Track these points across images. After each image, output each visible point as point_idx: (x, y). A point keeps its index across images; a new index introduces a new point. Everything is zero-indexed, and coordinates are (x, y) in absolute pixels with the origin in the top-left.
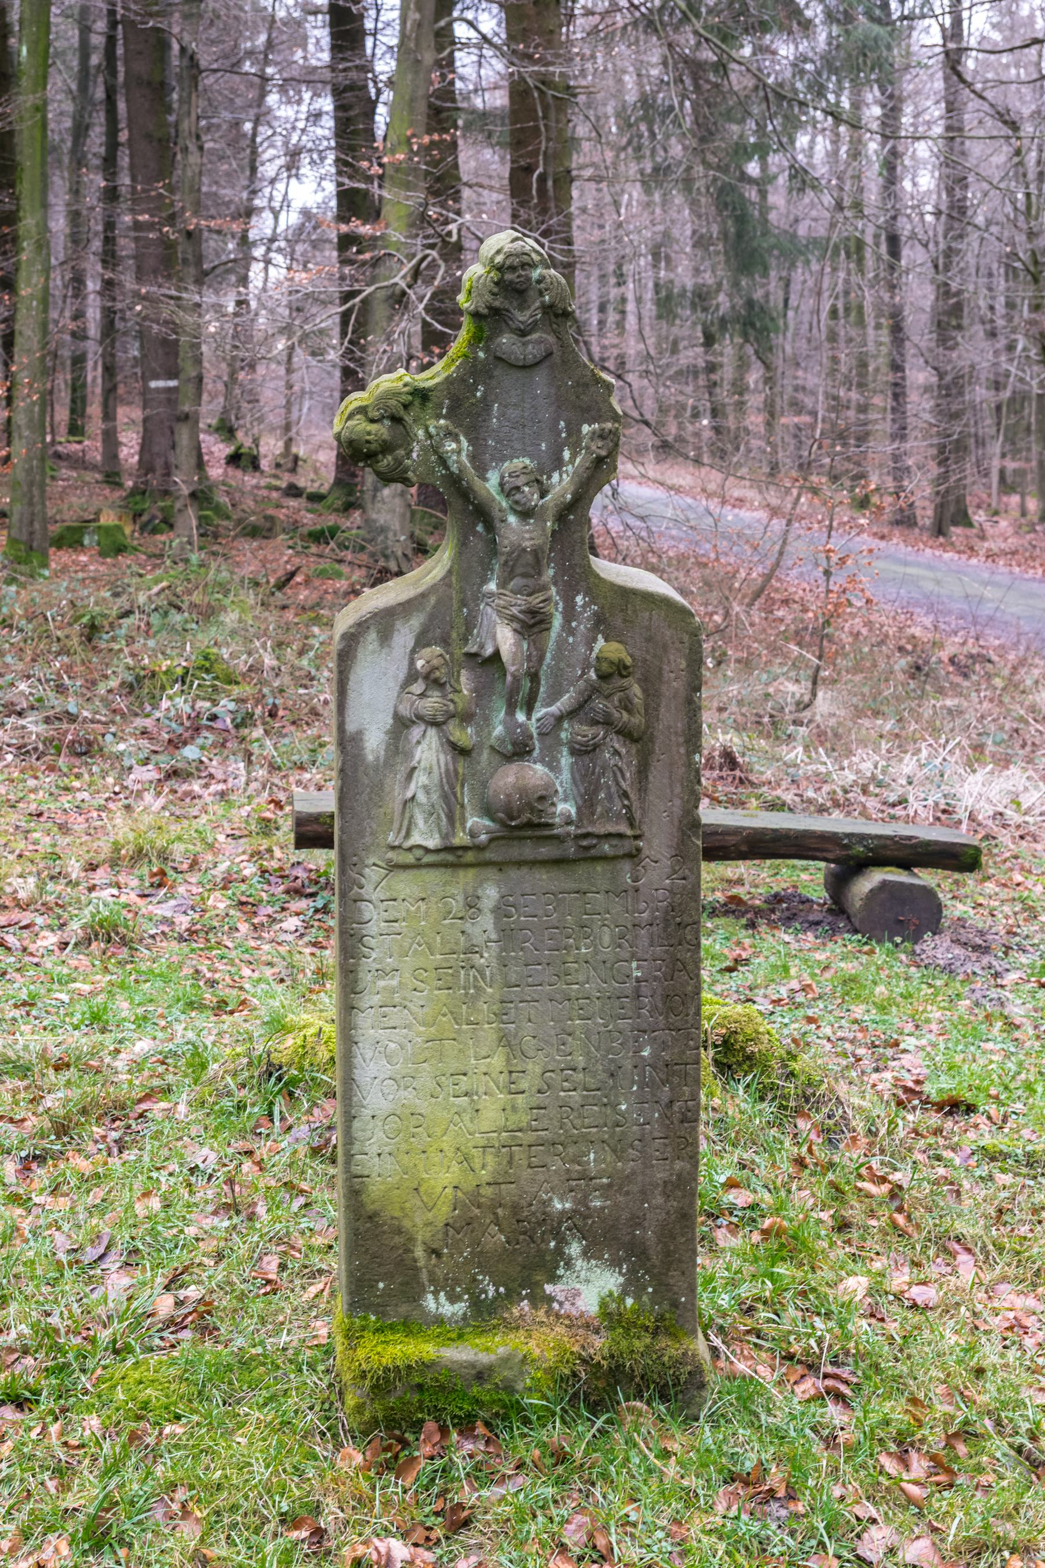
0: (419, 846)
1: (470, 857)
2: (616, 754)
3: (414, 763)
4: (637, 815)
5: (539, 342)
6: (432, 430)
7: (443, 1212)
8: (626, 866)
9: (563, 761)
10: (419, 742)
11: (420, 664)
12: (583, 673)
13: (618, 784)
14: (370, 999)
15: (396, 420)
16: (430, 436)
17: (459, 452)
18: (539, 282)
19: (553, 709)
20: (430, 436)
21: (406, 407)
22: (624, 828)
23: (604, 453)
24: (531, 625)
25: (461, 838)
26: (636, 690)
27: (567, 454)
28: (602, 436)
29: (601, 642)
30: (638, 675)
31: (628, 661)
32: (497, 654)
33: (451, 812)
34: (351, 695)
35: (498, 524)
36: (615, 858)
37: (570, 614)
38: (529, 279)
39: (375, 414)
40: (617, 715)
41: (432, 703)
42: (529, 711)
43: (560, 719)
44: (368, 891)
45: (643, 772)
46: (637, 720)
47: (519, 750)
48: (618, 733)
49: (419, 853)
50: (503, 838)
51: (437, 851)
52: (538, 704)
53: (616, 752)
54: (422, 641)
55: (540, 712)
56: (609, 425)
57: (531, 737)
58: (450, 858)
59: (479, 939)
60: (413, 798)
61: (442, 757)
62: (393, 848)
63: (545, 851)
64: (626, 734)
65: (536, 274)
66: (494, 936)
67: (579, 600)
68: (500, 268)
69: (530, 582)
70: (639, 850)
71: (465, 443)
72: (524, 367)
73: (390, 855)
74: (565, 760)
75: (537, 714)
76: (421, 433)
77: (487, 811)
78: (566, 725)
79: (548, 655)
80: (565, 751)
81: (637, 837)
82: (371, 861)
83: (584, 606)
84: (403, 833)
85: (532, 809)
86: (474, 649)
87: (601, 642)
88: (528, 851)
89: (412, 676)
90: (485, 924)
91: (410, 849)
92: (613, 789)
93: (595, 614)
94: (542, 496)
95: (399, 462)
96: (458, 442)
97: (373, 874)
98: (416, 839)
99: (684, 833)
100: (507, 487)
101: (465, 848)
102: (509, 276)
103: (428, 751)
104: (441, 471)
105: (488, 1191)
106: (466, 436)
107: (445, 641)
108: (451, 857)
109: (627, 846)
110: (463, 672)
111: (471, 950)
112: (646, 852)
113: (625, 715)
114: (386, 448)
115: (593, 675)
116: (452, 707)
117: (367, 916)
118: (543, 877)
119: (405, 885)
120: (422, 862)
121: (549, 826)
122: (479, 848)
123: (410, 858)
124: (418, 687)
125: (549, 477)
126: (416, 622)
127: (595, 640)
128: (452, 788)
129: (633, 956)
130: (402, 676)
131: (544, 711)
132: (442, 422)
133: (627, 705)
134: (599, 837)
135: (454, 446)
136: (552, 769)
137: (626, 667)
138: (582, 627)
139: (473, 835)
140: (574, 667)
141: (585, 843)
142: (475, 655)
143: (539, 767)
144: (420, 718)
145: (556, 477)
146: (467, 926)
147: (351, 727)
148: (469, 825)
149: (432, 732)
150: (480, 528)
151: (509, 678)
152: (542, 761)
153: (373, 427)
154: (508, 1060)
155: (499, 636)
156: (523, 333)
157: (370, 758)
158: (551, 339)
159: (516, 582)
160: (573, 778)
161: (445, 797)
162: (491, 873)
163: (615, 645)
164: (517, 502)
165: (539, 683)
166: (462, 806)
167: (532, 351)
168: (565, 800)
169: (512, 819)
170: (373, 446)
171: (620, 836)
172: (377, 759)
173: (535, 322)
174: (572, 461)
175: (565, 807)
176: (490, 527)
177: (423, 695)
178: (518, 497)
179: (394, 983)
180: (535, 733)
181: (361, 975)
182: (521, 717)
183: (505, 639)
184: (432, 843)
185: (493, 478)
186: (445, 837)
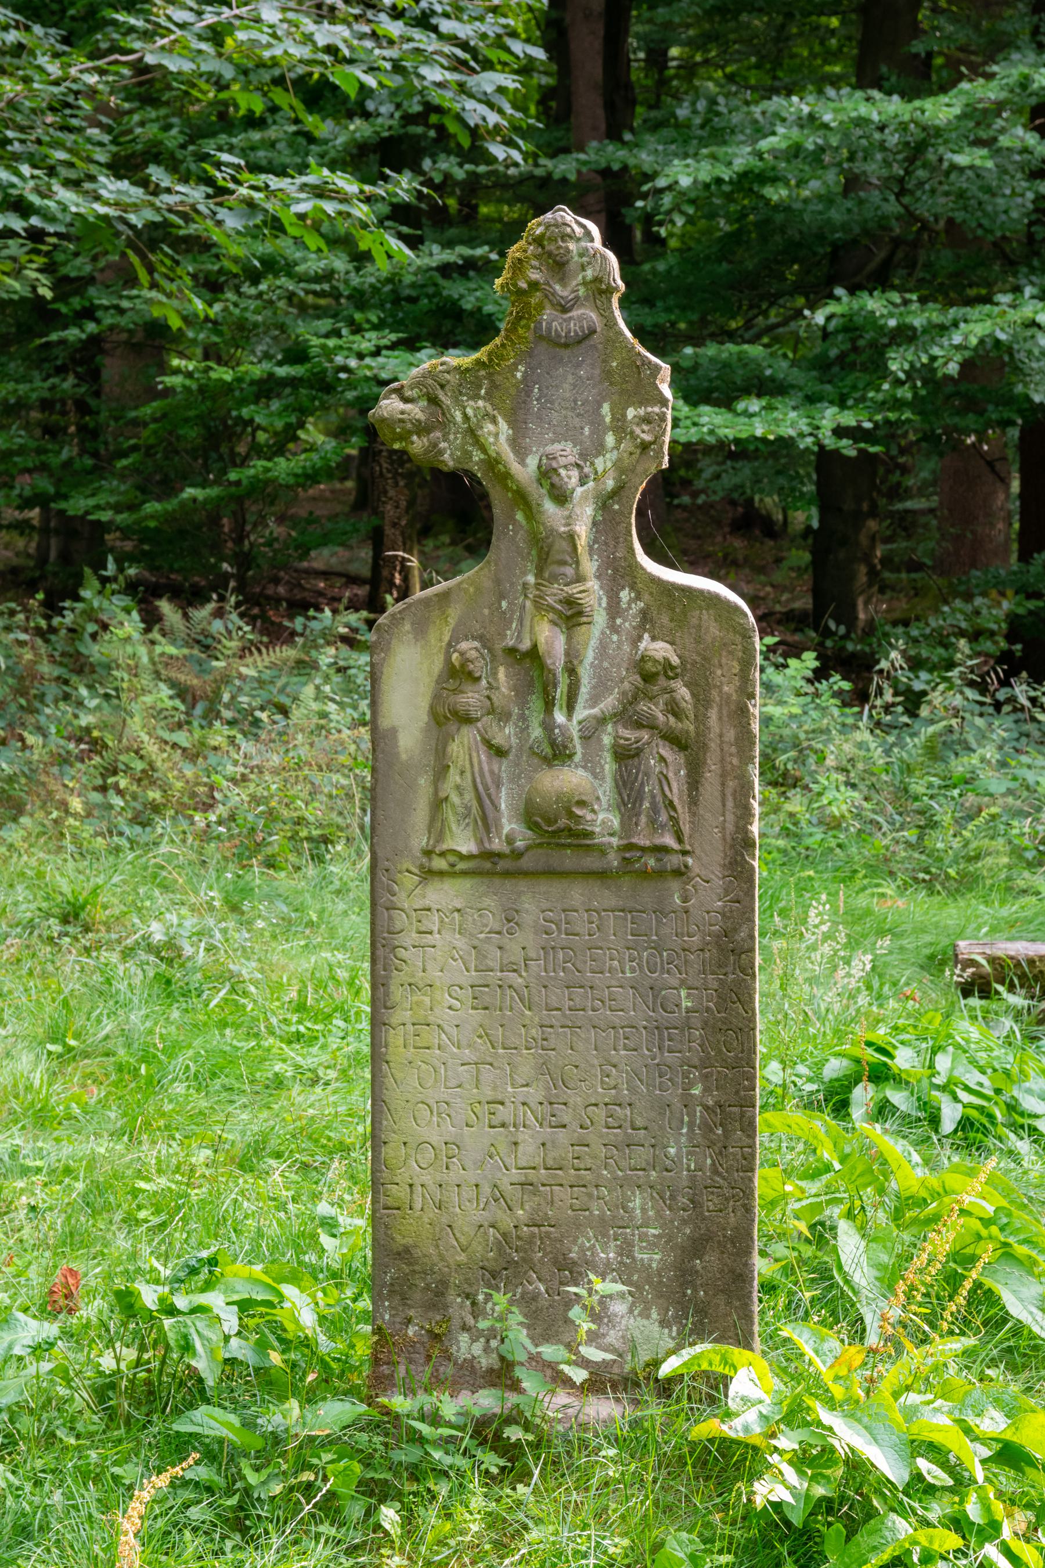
2: (665, 764)
4: (686, 829)
6: (470, 411)
8: (675, 885)
14: (400, 1015)
16: (466, 418)
17: (496, 435)
18: (581, 255)
19: (595, 711)
20: (466, 418)
23: (647, 438)
25: (497, 845)
26: (683, 692)
28: (647, 420)
31: (675, 660)
37: (614, 610)
40: (661, 717)
43: (602, 721)
44: (402, 899)
47: (557, 753)
49: (452, 859)
50: (540, 845)
51: (471, 857)
53: (662, 759)
55: (582, 712)
58: (488, 865)
67: (625, 595)
70: (686, 866)
71: (503, 425)
74: (609, 766)
76: (458, 416)
78: (610, 728)
81: (685, 853)
82: (405, 866)
83: (629, 603)
85: (571, 815)
88: (569, 859)
91: (442, 854)
92: (659, 799)
104: (477, 456)
106: (504, 417)
113: (672, 719)
117: (398, 926)
121: (589, 835)
127: (640, 638)
129: (683, 983)
132: (481, 403)
133: (674, 709)
136: (595, 776)
137: (672, 668)
138: (628, 624)
140: (619, 666)
143: (581, 772)
146: (506, 940)
150: (519, 516)
152: (585, 767)
157: (404, 757)
158: (593, 315)
170: (409, 426)
173: (577, 298)
180: (575, 734)
181: (392, 988)
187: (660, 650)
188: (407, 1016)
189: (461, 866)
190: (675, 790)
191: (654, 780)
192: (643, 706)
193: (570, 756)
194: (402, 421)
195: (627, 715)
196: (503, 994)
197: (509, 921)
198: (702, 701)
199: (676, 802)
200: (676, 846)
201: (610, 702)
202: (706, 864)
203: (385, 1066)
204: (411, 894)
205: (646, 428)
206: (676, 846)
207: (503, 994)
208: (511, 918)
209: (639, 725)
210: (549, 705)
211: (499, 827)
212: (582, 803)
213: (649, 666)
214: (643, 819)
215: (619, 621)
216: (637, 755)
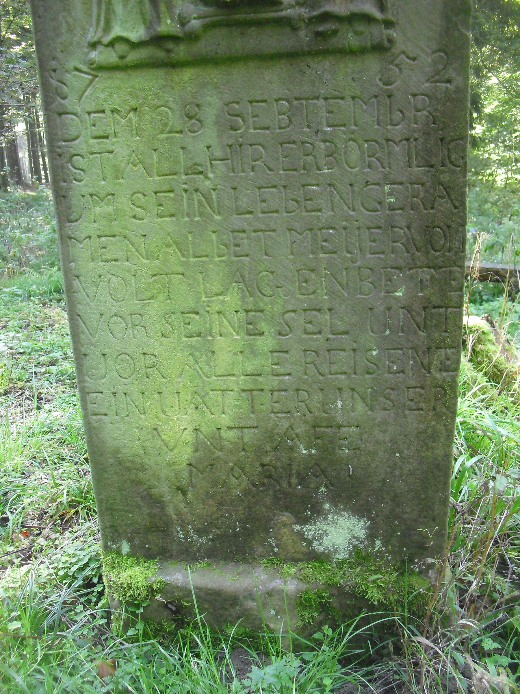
1: (181, 51)
7: (184, 454)
14: (85, 227)
25: (167, 26)
36: (363, 51)
51: (141, 44)
59: (202, 158)
63: (272, 41)
66: (218, 153)
70: (391, 41)
73: (94, 55)
81: (388, 24)
84: (102, 23)
90: (208, 139)
97: (75, 81)
98: (117, 31)
99: (447, 18)
105: (230, 435)
109: (378, 33)
112: (400, 46)
118: (273, 81)
119: (114, 91)
122: (191, 37)
134: (339, 19)
139: (183, 22)
146: (188, 139)
154: (243, 298)
162: (213, 75)
171: (368, 19)
179: (109, 209)
184: (137, 33)
186: (149, 26)
188: (92, 229)
189: (134, 56)
196: (191, 199)
197: (190, 118)
200: (378, 15)
203: (76, 282)
207: (191, 199)
208: (192, 116)
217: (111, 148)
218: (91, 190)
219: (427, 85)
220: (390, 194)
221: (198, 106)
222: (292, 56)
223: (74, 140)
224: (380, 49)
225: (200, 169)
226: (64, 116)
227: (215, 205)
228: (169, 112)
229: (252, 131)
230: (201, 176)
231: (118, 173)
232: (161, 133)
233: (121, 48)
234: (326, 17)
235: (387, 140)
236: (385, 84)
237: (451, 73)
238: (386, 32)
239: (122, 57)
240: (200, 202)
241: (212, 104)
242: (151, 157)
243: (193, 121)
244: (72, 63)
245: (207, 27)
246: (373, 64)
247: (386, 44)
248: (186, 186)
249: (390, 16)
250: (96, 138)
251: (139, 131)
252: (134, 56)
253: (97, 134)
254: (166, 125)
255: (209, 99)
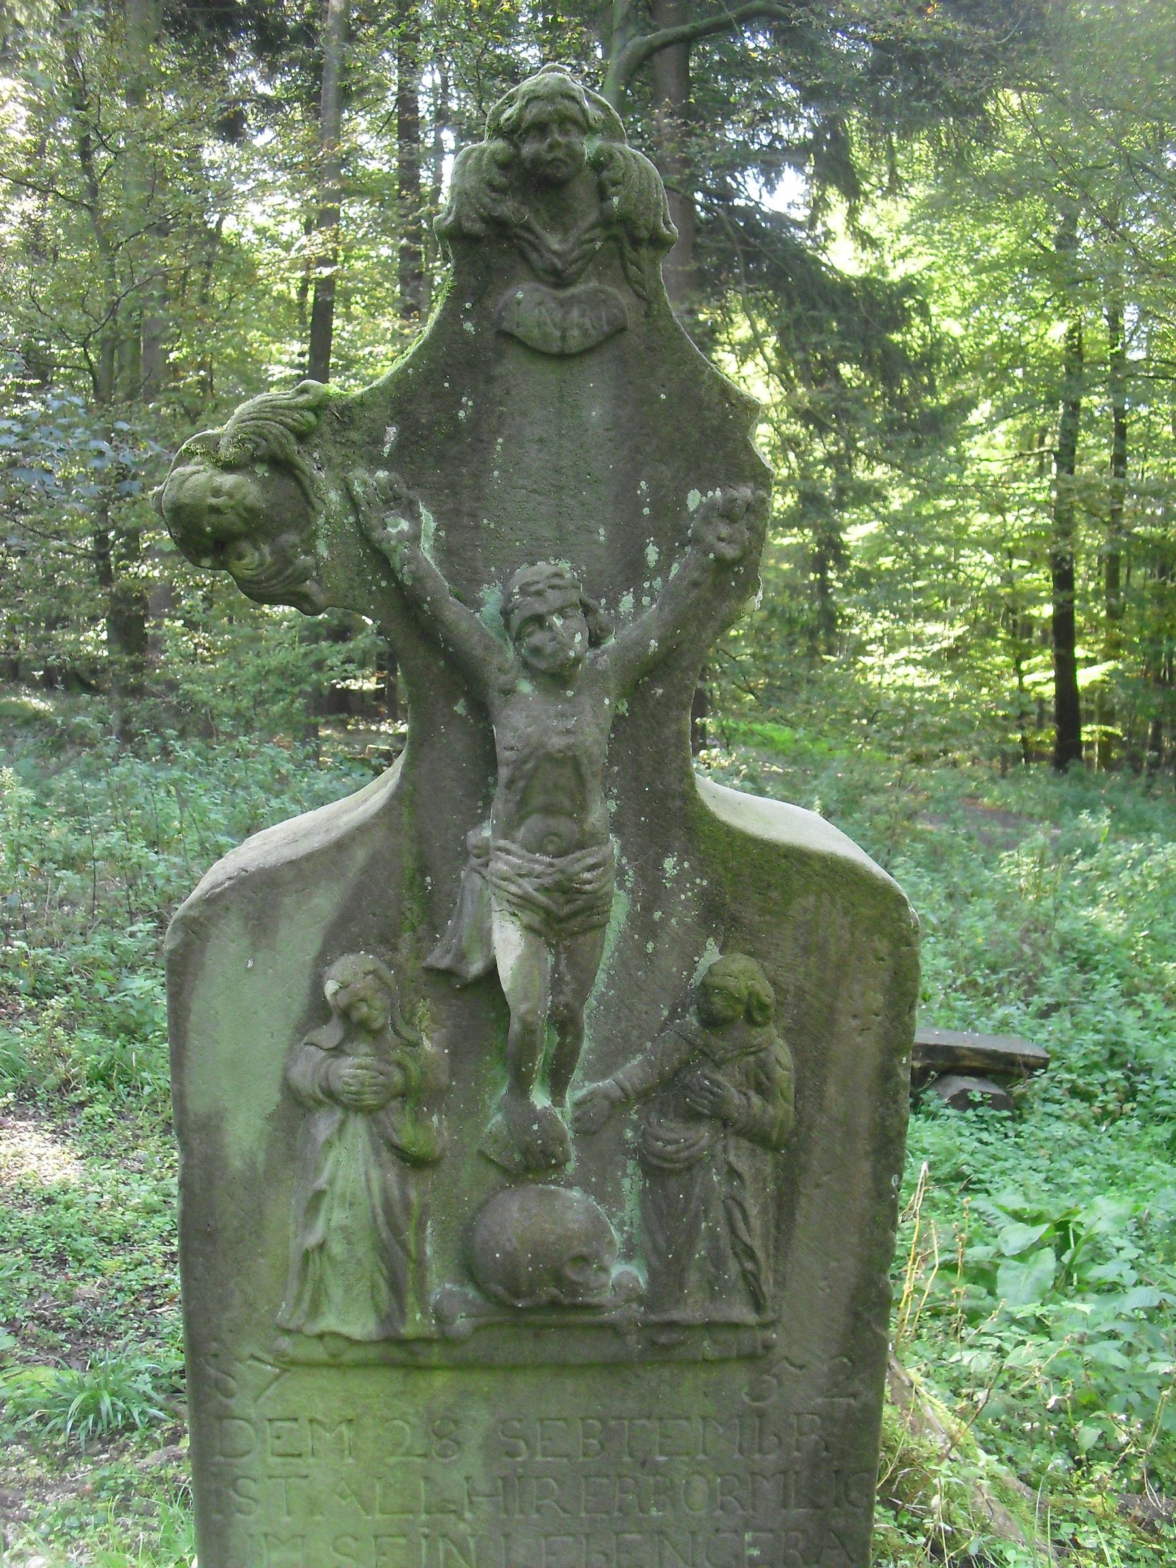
0: (335, 1335)
1: (435, 1354)
3: (321, 1183)
4: (768, 1288)
5: (594, 301)
6: (358, 489)
9: (626, 1183)
10: (329, 1144)
11: (330, 987)
12: (673, 1015)
13: (733, 1230)
15: (282, 466)
17: (415, 538)
21: (302, 437)
22: (742, 1313)
23: (730, 552)
24: (563, 920)
25: (416, 1323)
26: (782, 1052)
27: (652, 554)
28: (728, 513)
29: (711, 955)
30: (787, 1022)
31: (766, 992)
32: (491, 972)
33: (397, 1276)
34: (194, 1040)
35: (494, 697)
36: (723, 1361)
37: (651, 893)
38: (574, 155)
39: (227, 452)
40: (737, 1099)
41: (353, 1069)
42: (558, 1082)
44: (242, 1404)
45: (784, 1206)
46: (778, 1112)
47: (533, 1161)
48: (741, 1133)
51: (371, 1343)
52: (577, 1075)
53: (733, 1173)
54: (339, 939)
56: (745, 492)
57: (562, 1140)
58: (399, 1354)
60: (322, 1247)
61: (375, 1174)
62: (288, 1332)
64: (757, 1136)
65: (589, 147)
66: (483, 1486)
68: (512, 132)
69: (563, 825)
70: (768, 1347)
71: (428, 521)
72: (562, 357)
74: (630, 1183)
75: (572, 1096)
76: (334, 496)
77: (469, 1269)
79: (601, 977)
80: (631, 1166)
81: (764, 1326)
84: (305, 1305)
85: (558, 1279)
86: (445, 963)
87: (711, 955)
89: (319, 1011)
90: (467, 1468)
91: (321, 1336)
92: (725, 1243)
93: (703, 893)
94: (595, 641)
95: (284, 559)
96: (415, 518)
98: (329, 1322)
99: (857, 1316)
100: (516, 619)
101: (427, 1341)
102: (528, 149)
103: (349, 1164)
107: (387, 940)
108: (398, 1353)
110: (423, 1008)
111: (442, 1507)
112: (780, 1351)
113: (756, 1100)
114: (256, 525)
115: (692, 1020)
116: (397, 1077)
119: (319, 1396)
120: (341, 1356)
123: (319, 1352)
124: (330, 1034)
125: (614, 603)
126: (325, 901)
127: (699, 949)
128: (395, 1230)
129: (747, 1526)
130: (298, 1005)
131: (590, 1086)
132: (382, 474)
135: (404, 525)
136: (601, 1198)
137: (763, 1007)
139: (441, 1318)
141: (663, 1339)
142: (447, 975)
144: (331, 1095)
145: (627, 602)
147: (198, 1105)
148: (434, 1298)
149: (358, 1127)
150: (460, 708)
151: (515, 1026)
153: (228, 480)
155: (497, 937)
156: (559, 279)
157: (237, 1164)
159: (534, 823)
160: (645, 1218)
161: (383, 1252)
162: (483, 1382)
163: (740, 963)
164: (536, 651)
165: (579, 1037)
166: (421, 1263)
167: (580, 325)
168: (628, 1256)
169: (517, 1295)
171: (736, 1326)
172: (252, 1166)
174: (663, 567)
175: (624, 1272)
176: (481, 710)
177: (337, 1051)
178: (538, 638)
182: (540, 1099)
183: (509, 945)
185: (491, 597)
186: (386, 1320)
187: (742, 973)
190: (756, 1223)
191: (718, 1213)
192: (702, 1075)
193: (560, 1166)
194: (215, 510)
195: (672, 1092)
198: (812, 1066)
199: (756, 1244)
201: (633, 1070)
202: (804, 1338)
204: (263, 1400)
205: (724, 530)
206: (751, 1318)
208: (443, 1433)
209: (693, 1117)
210: (521, 1086)
211: (422, 1296)
212: (583, 1260)
213: (718, 1003)
214: (693, 1277)
215: (657, 915)
216: (689, 1168)
217: (304, 1472)
218: (267, 1529)
219: (819, 1400)
220: (753, 1544)
221: (456, 1422)
222: (612, 1366)
223: (242, 1455)
224: (750, 1358)
225: (452, 1507)
226: (226, 1423)
227: (473, 1556)
228: (407, 1427)
229: (539, 1458)
230: (452, 1516)
231: (313, 1506)
232: (392, 1454)
233: (334, 1345)
234: (671, 1325)
235: (753, 1474)
236: (754, 1400)
237: (857, 1385)
238: (760, 1335)
239: (334, 1356)
240: (448, 1553)
241: (479, 1420)
242: (372, 1487)
243: (445, 1441)
244: (247, 1349)
245: (477, 1329)
246: (740, 1378)
247: (760, 1351)
248: (426, 1530)
249: (770, 1316)
250: (280, 1455)
251: (353, 1450)
252: (350, 1355)
253: (281, 1451)
254: (399, 1445)
255: (473, 1413)
